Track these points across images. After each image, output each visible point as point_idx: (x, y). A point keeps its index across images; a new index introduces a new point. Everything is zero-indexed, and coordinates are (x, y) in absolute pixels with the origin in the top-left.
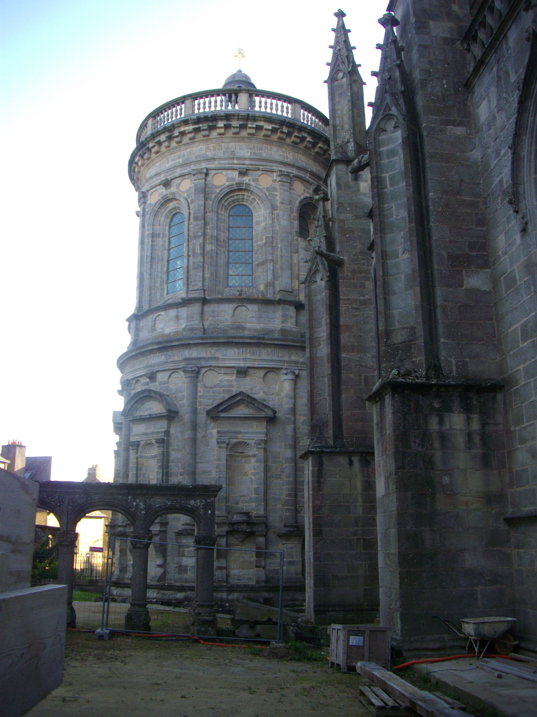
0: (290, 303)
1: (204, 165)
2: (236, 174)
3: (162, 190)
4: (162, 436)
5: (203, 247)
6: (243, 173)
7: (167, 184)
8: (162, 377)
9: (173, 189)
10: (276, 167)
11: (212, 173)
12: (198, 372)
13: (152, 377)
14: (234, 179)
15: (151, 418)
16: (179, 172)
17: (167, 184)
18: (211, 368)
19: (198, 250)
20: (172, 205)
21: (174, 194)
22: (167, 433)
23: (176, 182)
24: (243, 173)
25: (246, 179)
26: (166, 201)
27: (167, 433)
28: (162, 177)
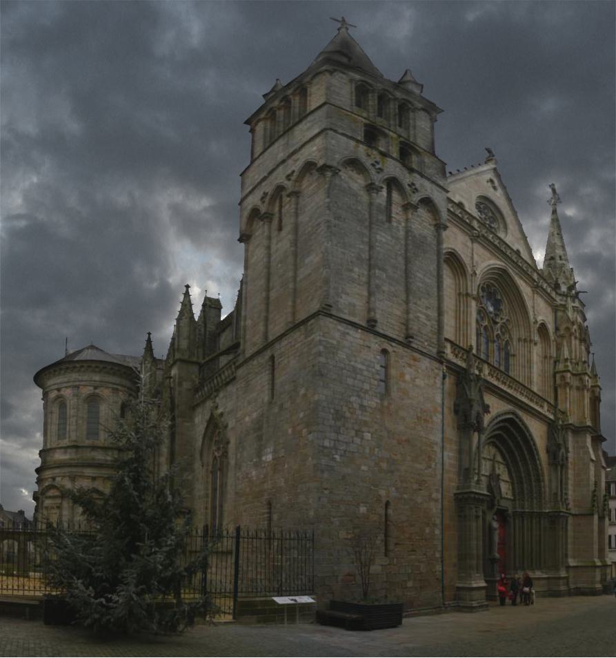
0: (116, 449)
1: (77, 383)
2: (92, 388)
3: (56, 392)
4: (58, 505)
5: (77, 421)
6: (96, 388)
7: (59, 390)
8: (58, 479)
9: (62, 392)
10: (111, 385)
11: (81, 387)
12: (75, 478)
13: (54, 479)
14: (91, 390)
15: (54, 497)
16: (66, 385)
17: (59, 390)
18: (80, 476)
19: (74, 423)
20: (61, 399)
21: (62, 395)
22: (61, 504)
23: (63, 389)
24: (96, 388)
25: (97, 391)
26: (58, 397)
27: (61, 504)
28: (56, 387)
